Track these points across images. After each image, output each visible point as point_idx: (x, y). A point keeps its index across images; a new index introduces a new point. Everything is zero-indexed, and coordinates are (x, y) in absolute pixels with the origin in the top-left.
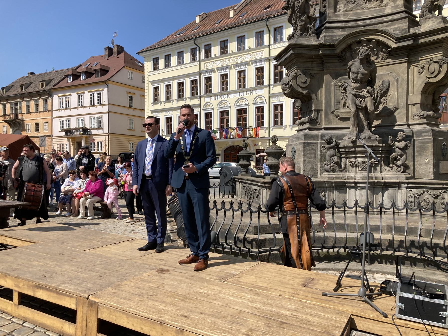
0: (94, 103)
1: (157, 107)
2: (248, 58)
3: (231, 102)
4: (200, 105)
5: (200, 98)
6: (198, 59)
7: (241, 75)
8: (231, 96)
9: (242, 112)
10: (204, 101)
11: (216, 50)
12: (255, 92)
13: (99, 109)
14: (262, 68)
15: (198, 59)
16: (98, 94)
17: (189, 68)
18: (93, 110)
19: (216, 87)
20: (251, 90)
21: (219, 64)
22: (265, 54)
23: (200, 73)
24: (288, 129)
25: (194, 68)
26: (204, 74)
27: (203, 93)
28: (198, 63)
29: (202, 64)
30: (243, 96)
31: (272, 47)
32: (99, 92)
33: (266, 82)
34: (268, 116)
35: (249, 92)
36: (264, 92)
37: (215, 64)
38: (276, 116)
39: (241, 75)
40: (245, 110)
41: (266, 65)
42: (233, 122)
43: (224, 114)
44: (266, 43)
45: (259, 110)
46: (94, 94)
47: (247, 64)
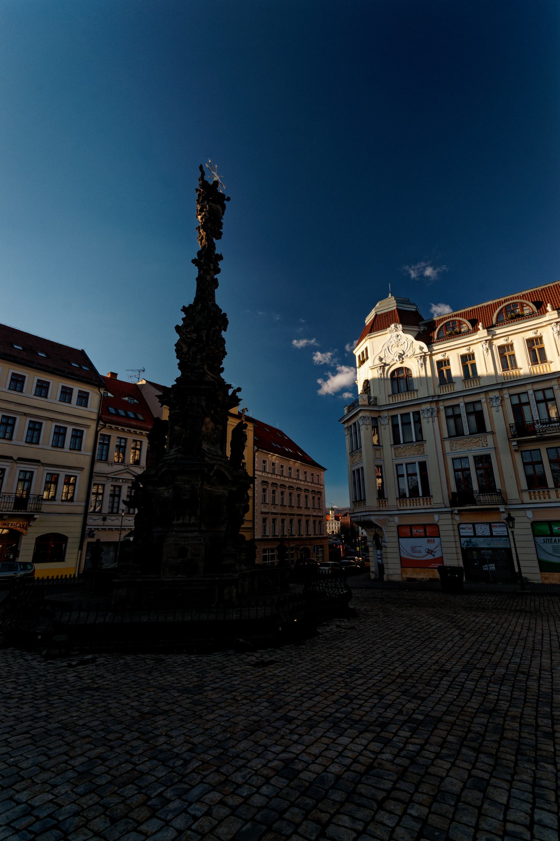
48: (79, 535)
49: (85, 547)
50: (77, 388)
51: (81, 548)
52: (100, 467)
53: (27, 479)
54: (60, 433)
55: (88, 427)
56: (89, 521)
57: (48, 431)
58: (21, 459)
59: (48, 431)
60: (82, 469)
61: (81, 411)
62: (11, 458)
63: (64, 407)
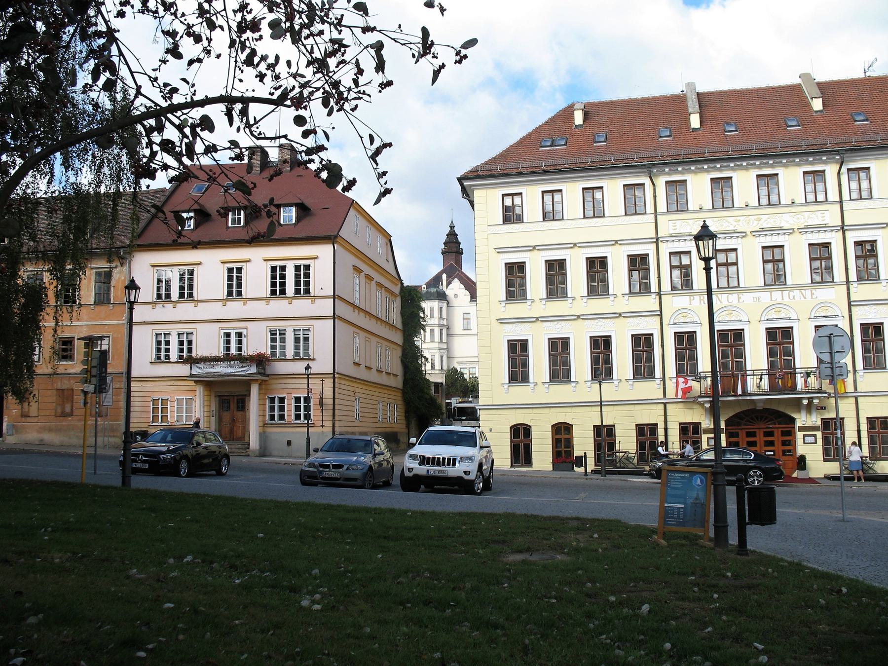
3: (733, 310)
8: (747, 297)
12: (812, 294)
13: (302, 307)
14: (827, 246)
15: (650, 208)
16: (297, 268)
18: (279, 307)
20: (800, 287)
25: (642, 227)
26: (670, 244)
30: (779, 301)
33: (839, 274)
35: (796, 293)
40: (787, 333)
41: (835, 239)
46: (283, 268)
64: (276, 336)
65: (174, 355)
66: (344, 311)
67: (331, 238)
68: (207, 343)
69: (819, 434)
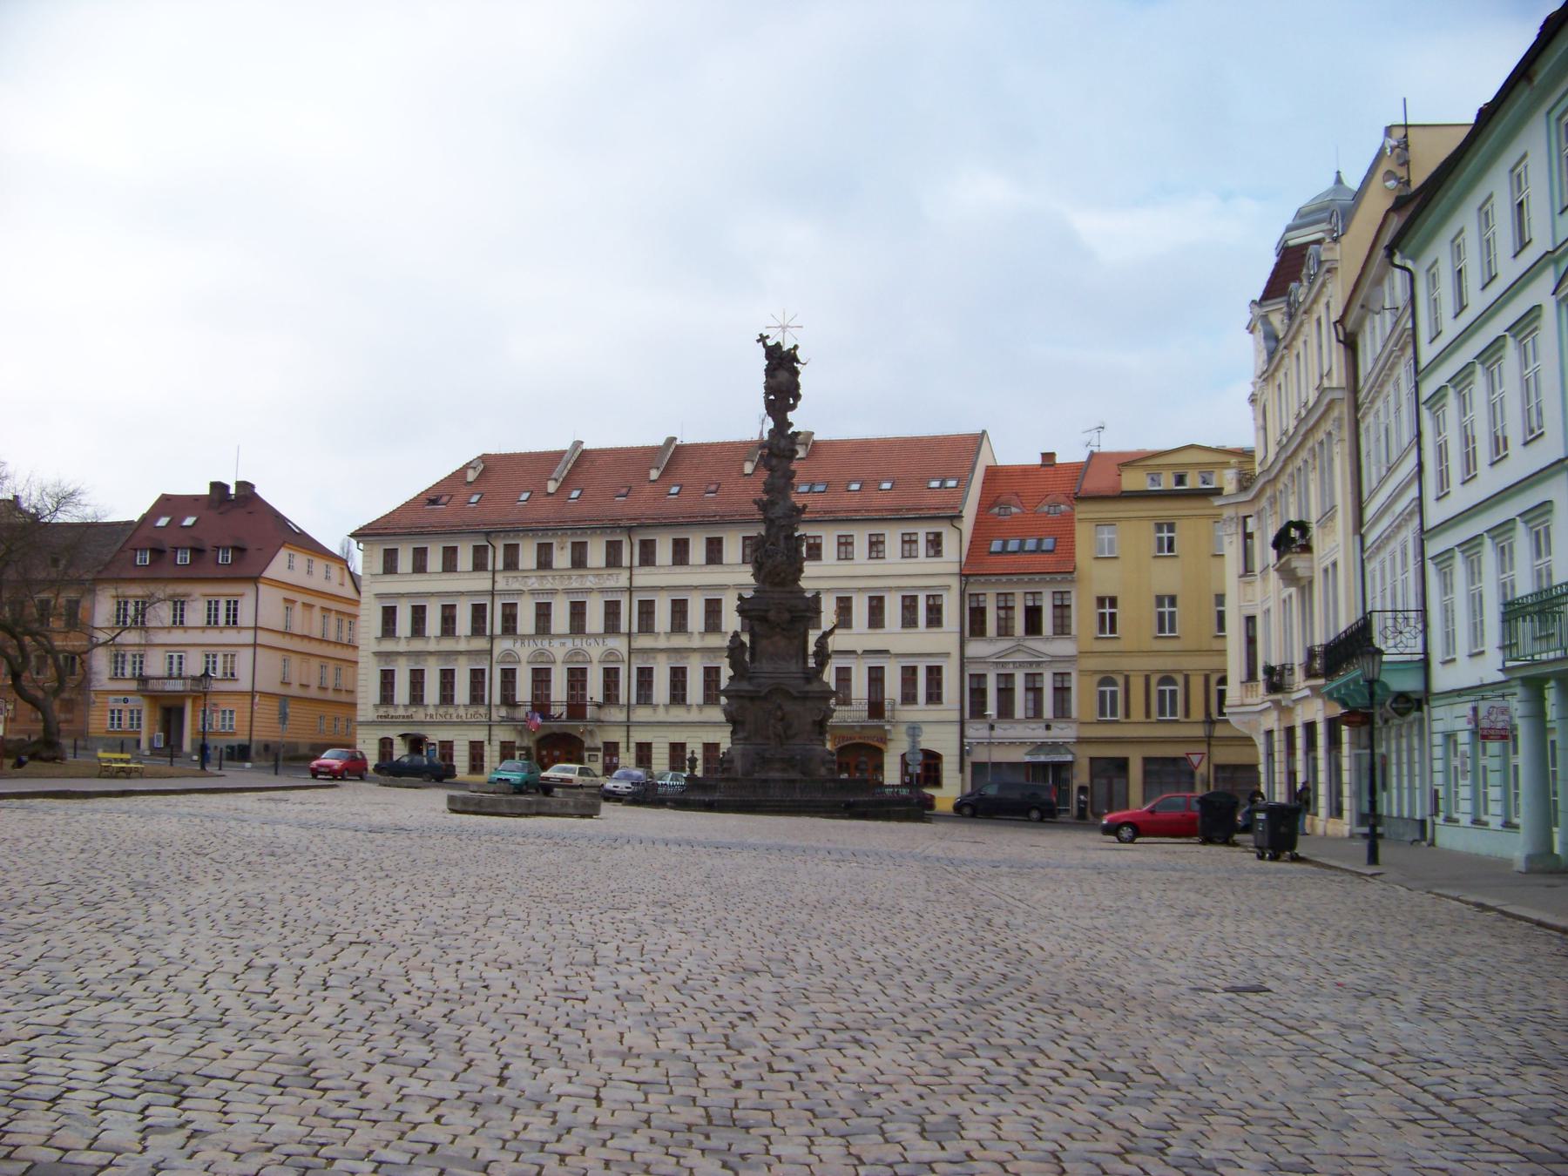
0: (216, 622)
1: (389, 646)
2: (590, 582)
4: (491, 652)
5: (492, 638)
6: (490, 567)
7: (578, 611)
8: (556, 643)
9: (577, 678)
10: (502, 645)
11: (528, 556)
13: (230, 636)
14: (618, 603)
17: (468, 582)
18: (213, 636)
19: (526, 620)
21: (533, 583)
22: (622, 580)
23: (492, 593)
24: (661, 710)
25: (482, 582)
27: (498, 630)
28: (490, 575)
29: (499, 577)
31: (635, 571)
32: (232, 599)
33: (624, 628)
34: (627, 688)
35: (592, 641)
36: (619, 644)
37: (524, 586)
38: (640, 684)
39: (578, 611)
40: (583, 671)
42: (559, 690)
43: (541, 678)
44: (625, 561)
45: (611, 676)
47: (589, 591)
48: (957, 751)
49: (968, 770)
50: (922, 532)
51: (962, 770)
52: (975, 648)
53: (876, 676)
54: (909, 605)
55: (948, 588)
56: (970, 732)
57: (893, 610)
58: (866, 652)
59: (893, 610)
60: (947, 655)
61: (935, 565)
62: (854, 652)
63: (910, 567)
64: (210, 659)
65: (128, 671)
66: (263, 638)
67: (255, 580)
68: (156, 665)
69: (600, 755)
